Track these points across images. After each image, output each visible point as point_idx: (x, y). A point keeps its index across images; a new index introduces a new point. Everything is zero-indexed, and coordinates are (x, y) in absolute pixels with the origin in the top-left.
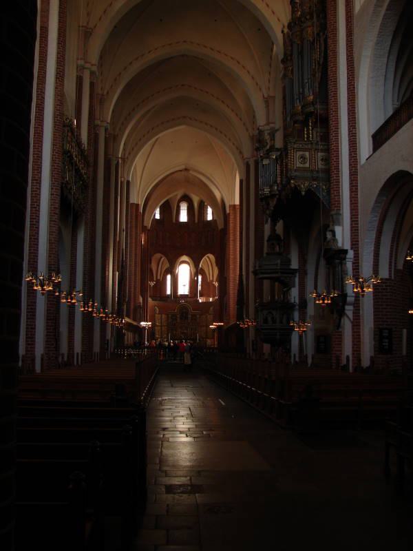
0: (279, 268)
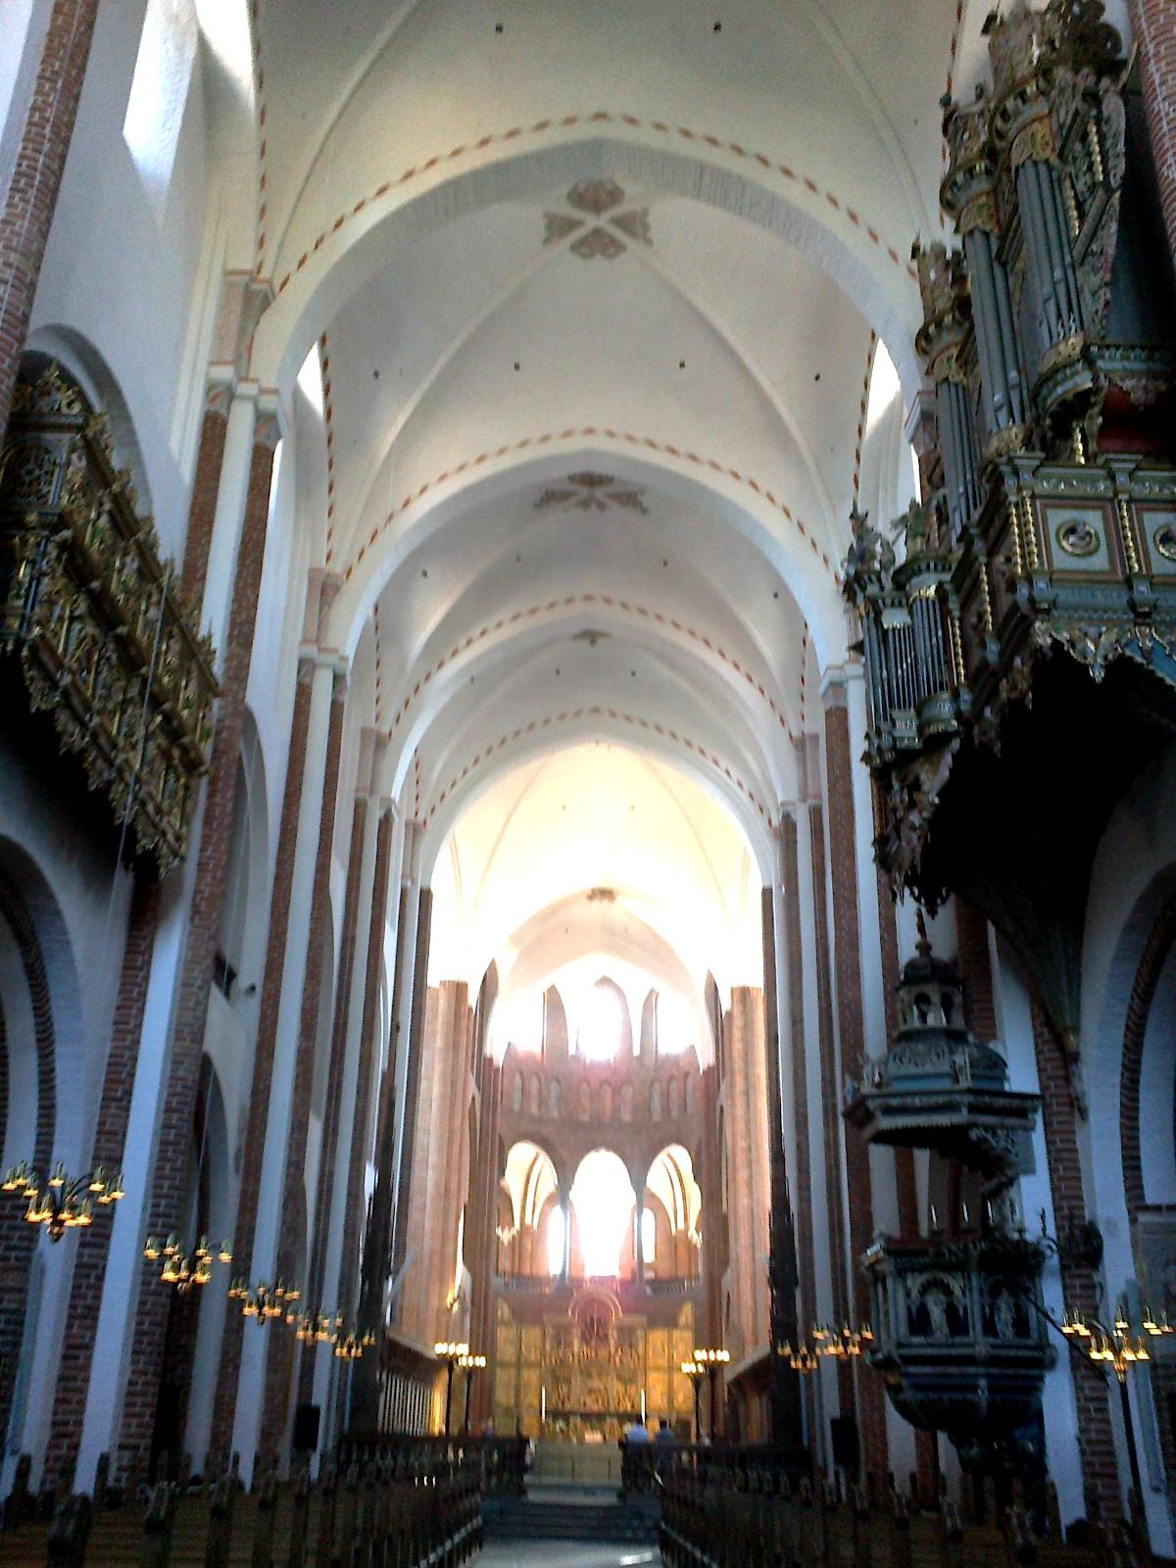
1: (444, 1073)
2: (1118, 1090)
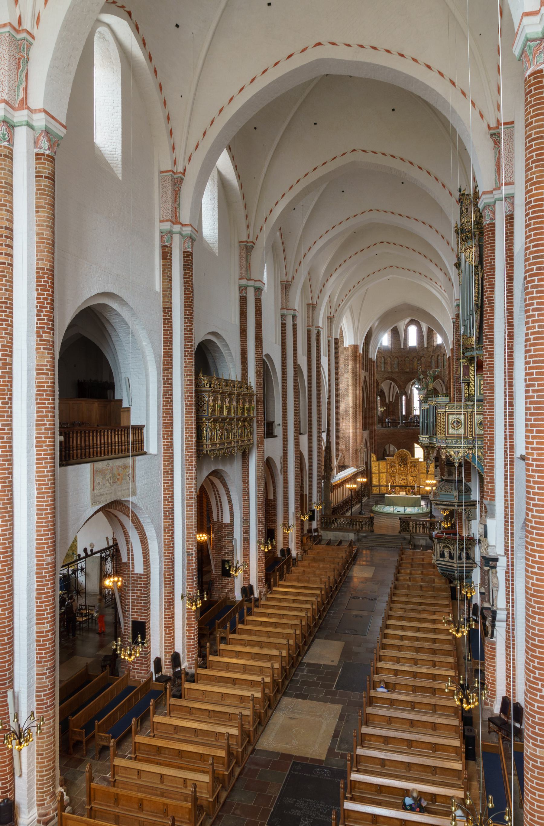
1: (353, 377)
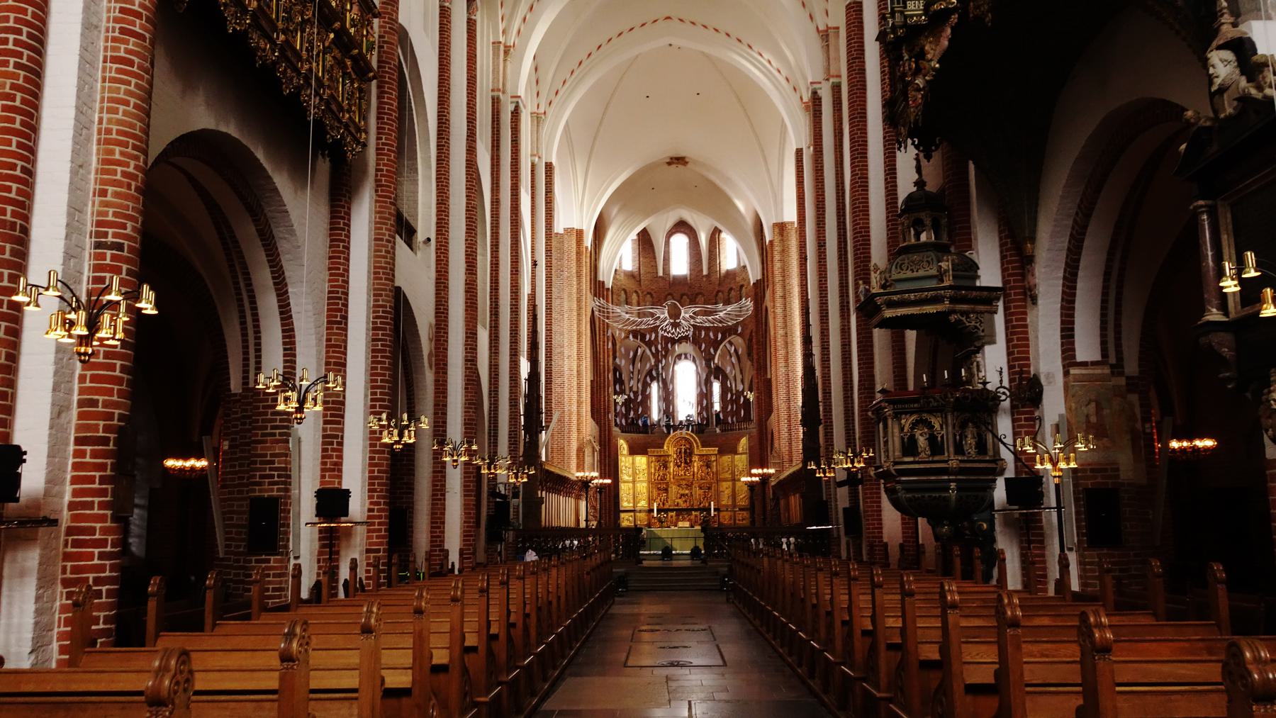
0: (946, 284)
2: (1061, 282)
